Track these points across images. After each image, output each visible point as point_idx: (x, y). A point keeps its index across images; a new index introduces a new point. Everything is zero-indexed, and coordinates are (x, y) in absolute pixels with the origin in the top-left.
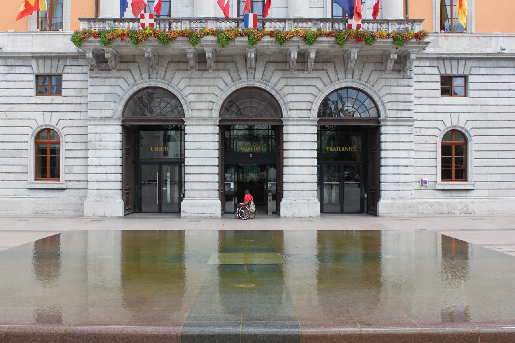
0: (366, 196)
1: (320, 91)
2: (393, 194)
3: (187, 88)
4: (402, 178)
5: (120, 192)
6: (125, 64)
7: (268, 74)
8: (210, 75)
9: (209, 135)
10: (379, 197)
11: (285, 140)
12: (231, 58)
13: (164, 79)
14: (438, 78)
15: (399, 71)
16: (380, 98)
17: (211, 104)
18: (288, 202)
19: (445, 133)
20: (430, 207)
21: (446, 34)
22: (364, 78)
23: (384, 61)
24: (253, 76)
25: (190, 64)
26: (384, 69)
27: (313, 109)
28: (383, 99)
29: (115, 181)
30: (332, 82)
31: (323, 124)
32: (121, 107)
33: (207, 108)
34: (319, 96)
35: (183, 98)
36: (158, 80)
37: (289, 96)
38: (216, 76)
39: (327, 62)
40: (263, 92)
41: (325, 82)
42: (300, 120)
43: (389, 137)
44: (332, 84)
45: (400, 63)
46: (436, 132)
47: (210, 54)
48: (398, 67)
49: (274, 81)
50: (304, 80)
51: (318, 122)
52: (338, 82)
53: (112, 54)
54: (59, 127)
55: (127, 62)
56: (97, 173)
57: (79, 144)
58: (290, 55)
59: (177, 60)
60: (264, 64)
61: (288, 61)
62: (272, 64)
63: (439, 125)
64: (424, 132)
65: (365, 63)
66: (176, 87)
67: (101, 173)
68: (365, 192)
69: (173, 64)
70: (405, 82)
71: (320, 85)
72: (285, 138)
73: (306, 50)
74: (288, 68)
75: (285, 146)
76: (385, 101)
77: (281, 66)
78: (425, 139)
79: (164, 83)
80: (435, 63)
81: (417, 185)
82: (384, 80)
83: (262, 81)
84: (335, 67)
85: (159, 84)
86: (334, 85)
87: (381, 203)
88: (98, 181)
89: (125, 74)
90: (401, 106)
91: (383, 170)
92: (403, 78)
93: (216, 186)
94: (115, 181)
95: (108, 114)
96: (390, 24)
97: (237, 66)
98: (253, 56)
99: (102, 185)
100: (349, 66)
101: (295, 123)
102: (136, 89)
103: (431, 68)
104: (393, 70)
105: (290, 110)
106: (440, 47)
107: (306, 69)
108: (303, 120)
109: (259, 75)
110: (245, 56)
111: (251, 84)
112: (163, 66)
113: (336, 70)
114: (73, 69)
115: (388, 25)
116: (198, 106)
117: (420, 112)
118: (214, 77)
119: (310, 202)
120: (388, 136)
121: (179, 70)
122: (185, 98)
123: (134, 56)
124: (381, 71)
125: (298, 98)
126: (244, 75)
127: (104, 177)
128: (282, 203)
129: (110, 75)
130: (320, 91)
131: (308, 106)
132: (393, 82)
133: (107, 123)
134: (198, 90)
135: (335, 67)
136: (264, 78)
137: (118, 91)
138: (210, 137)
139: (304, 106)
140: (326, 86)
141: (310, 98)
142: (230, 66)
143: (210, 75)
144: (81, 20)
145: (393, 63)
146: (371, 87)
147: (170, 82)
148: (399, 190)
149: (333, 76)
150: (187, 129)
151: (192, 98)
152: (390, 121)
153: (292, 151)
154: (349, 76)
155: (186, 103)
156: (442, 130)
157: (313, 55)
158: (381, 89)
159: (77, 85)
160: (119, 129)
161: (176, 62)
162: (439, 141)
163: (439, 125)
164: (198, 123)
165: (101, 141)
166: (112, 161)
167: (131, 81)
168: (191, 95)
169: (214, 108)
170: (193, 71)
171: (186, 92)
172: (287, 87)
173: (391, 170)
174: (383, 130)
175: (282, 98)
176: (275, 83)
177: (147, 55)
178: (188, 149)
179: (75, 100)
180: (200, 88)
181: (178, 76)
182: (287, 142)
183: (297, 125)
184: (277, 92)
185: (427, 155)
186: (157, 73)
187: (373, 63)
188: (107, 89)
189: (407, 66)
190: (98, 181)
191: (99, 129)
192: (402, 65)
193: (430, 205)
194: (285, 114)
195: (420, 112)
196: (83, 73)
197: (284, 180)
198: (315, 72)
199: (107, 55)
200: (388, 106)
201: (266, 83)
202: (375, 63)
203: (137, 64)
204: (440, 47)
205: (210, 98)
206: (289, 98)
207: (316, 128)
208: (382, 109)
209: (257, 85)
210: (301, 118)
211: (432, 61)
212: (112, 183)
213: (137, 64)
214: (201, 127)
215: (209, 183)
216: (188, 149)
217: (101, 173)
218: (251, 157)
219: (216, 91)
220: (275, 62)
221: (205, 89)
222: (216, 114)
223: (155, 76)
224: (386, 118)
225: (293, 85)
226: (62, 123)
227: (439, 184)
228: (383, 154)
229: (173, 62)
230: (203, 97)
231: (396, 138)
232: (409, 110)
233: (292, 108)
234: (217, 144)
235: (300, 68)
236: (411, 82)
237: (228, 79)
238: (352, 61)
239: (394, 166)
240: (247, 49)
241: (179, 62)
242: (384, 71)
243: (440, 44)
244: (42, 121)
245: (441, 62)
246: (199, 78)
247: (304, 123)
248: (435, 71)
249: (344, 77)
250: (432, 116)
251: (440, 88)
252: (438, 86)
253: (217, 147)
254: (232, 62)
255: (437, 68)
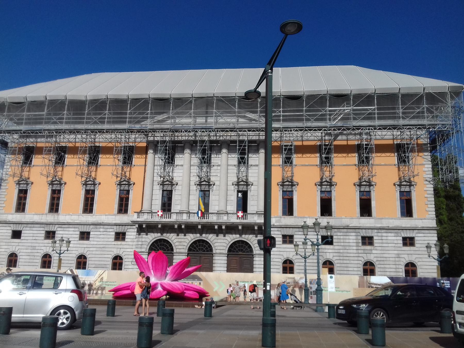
46: (280, 260)
54: (123, 255)
75: (214, 265)
114: (131, 230)
116: (180, 247)
134: (180, 240)
144: (135, 212)
151: (177, 244)
159: (132, 237)
171: (175, 241)
179: (130, 243)
206: (216, 244)
210: (220, 254)
226: (124, 253)
230: (181, 244)
244: (116, 252)
248: (279, 233)
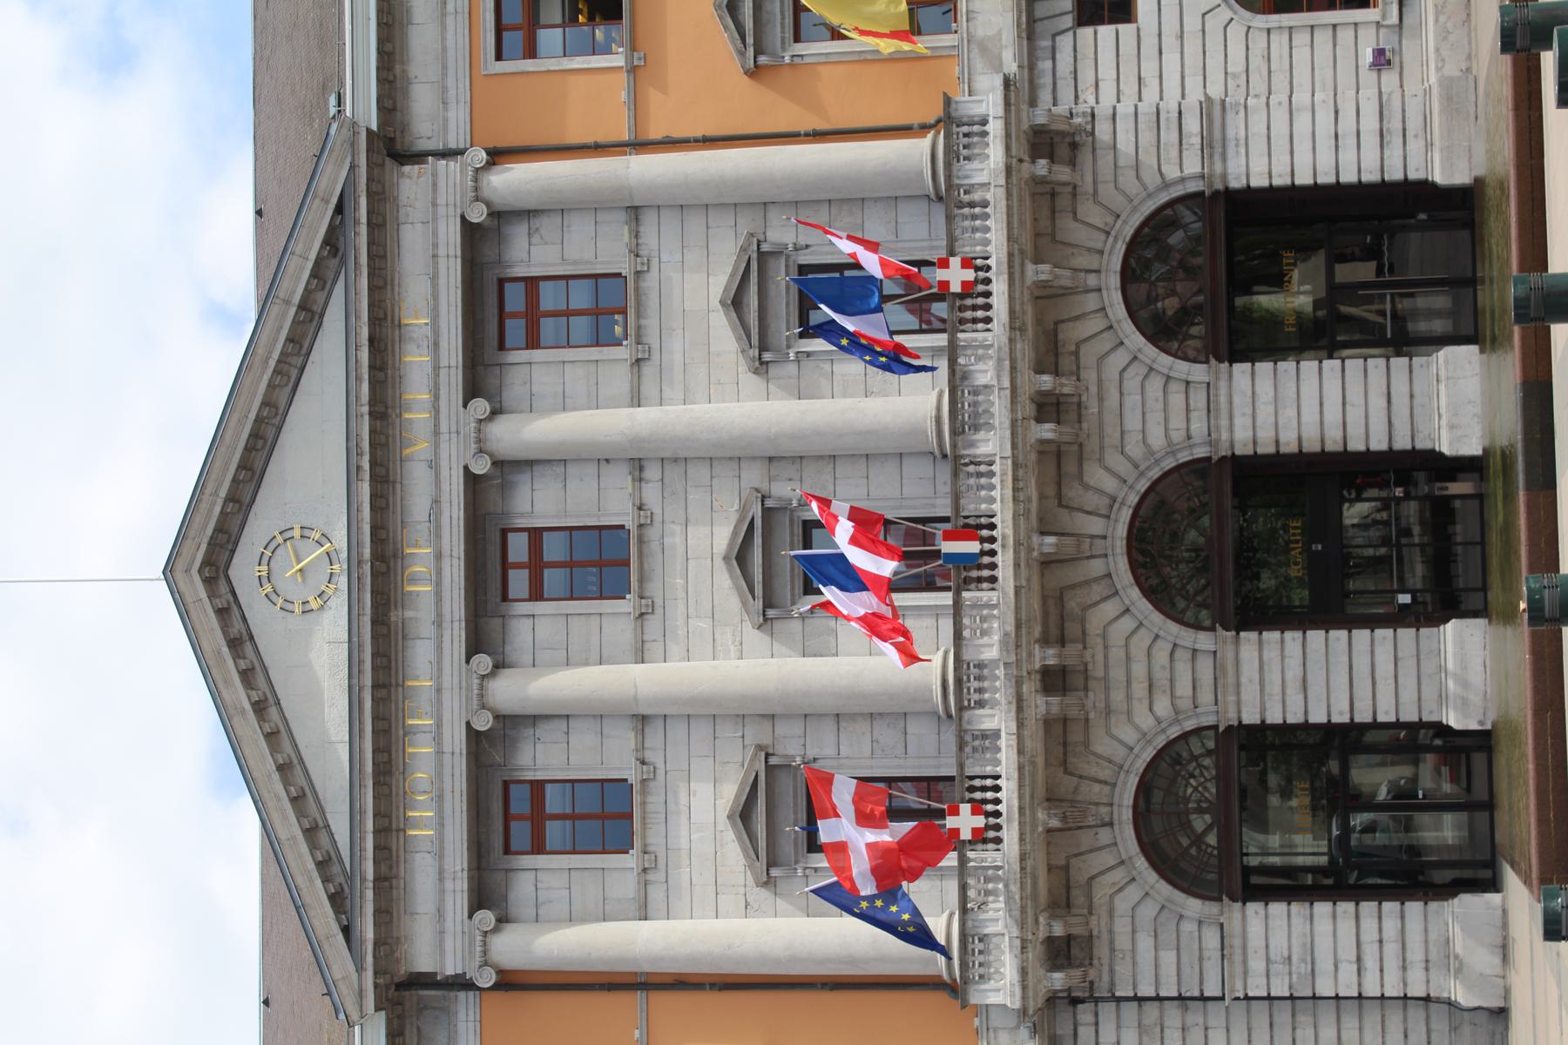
0: (1422, 216)
1: (1135, 358)
2: (1415, 146)
3: (1137, 720)
4: (1370, 123)
5: (1433, 905)
6: (1075, 892)
7: (1092, 501)
8: (1100, 658)
9: (1265, 657)
10: (1425, 186)
11: (1271, 450)
12: (1051, 602)
13: (1114, 785)
14: (1086, 32)
15: (1074, 146)
16: (1150, 196)
17: (1179, 653)
18: (1444, 433)
19: (1237, 7)
20: (1452, 38)
21: (962, 18)
22: (1096, 240)
23: (1047, 188)
24: (1098, 542)
25: (1074, 712)
26: (1070, 189)
27: (1184, 377)
28: (1151, 188)
29: (1402, 917)
30: (1111, 327)
31: (1224, 347)
32: (1194, 906)
33: (1189, 665)
34: (1148, 361)
35: (1164, 731)
36: (1116, 801)
37: (1151, 441)
38: (1099, 640)
39: (1056, 343)
40: (1142, 513)
41: (1108, 346)
42: (1217, 410)
43: (1257, 165)
44: (1115, 326)
45: (1052, 145)
46: (1236, 33)
47: (1051, 652)
48: (1063, 151)
49: (1110, 484)
50: (1106, 404)
51: (1221, 361)
52: (1109, 310)
53: (1052, 917)
55: (1068, 888)
56: (1381, 970)
57: (1298, 1032)
58: (1042, 442)
59: (1061, 748)
60: (1064, 512)
61: (1053, 448)
62: (1065, 490)
63: (1215, 23)
64: (1237, 65)
65: (1054, 240)
66: (1136, 751)
67: (1381, 960)
68: (1414, 216)
69: (1071, 759)
70: (1103, 130)
71: (1119, 359)
72: (1266, 448)
73: (1032, 400)
74: (1075, 448)
75: (1289, 447)
76: (1159, 180)
77: (1070, 467)
78: (1257, 61)
79: (1125, 783)
80: (1046, 43)
81: (1390, 78)
82: (1101, 187)
83: (1113, 516)
84: (1069, 320)
85: (1126, 796)
86: (1119, 322)
87: (1439, 178)
88: (1404, 968)
89: (1100, 894)
90: (1170, 136)
91: (1349, 177)
92: (1093, 133)
93: (1406, 634)
94: (1402, 917)
95: (1211, 939)
96: (957, 181)
97: (1073, 587)
98: (1051, 540)
99: (1416, 954)
100: (1067, 283)
101: (1224, 422)
102: (1141, 863)
103: (1058, 56)
104: (1072, 163)
105: (1189, 437)
106: (1000, 31)
107: (1075, 400)
108: (1217, 402)
109: (1095, 526)
110: (1047, 563)
111: (1120, 546)
112: (1076, 788)
113: (1077, 318)
115: (960, 186)
116: (1184, 688)
117: (1183, 77)
118: (1106, 647)
119: (1442, 374)
120: (1254, 169)
121: (1086, 744)
122: (1163, 725)
123: (1049, 870)
124: (1074, 195)
125: (1155, 417)
126: (1096, 567)
127: (1391, 949)
128: (1446, 450)
129: (1105, 936)
130: (1135, 358)
131: (1176, 389)
132: (1105, 161)
133: (1237, 942)
134: (1140, 689)
135: (1069, 320)
136: (1103, 512)
137: (1148, 911)
138: (1272, 653)
139: (1177, 400)
140: (1122, 343)
141: (1155, 385)
142: (1072, 604)
143: (1100, 658)
145: (1056, 168)
146: (1119, 222)
147: (1121, 767)
148: (1404, 130)
149: (1094, 325)
150: (1250, 717)
151: (1163, 706)
152: (1212, 164)
153: (1303, 427)
154: (1092, 280)
155: (1177, 721)
156: (1228, 14)
157: (1046, 382)
158: (1124, 194)
160: (1254, 908)
161: (1065, 754)
162: (1262, 21)
163: (1215, 23)
164: (1231, 689)
165: (1289, 958)
166: (1346, 927)
167: (1118, 875)
168: (1155, 708)
169: (1189, 644)
170: (1089, 703)
171: (1145, 721)
172: (1127, 449)
173: (1348, 157)
174: (1236, 183)
175: (1157, 461)
176: (1115, 485)
177: (1055, 823)
178: (1306, 712)
180: (1135, 685)
181: (1102, 745)
182: (1277, 442)
183: (1231, 418)
184: (1142, 474)
185: (1302, 54)
186: (1097, 804)
187: (1053, 219)
188: (1145, 943)
189: (1064, 127)
190: (1404, 968)
191: (1257, 965)
192: (1057, 139)
193: (1445, 39)
194: (1201, 452)
195: (1183, 77)
196: (1097, 1024)
197: (1384, 447)
198: (1083, 374)
199: (1058, 930)
200: (1172, 172)
201: (1116, 506)
202: (1053, 212)
203: (1073, 861)
204: (1000, 31)
205: (1161, 655)
206: (1157, 439)
207: (1236, 366)
208: (1180, 187)
209: (1122, 530)
211: (1039, 53)
212: (1408, 926)
213: (1073, 861)
214: (1243, 680)
215: (1400, 654)
216: (1306, 712)
217: (1381, 960)
218: (1320, 547)
219: (1142, 641)
220: (1059, 484)
221: (1139, 669)
222: (1204, 641)
223: (1104, 810)
224: (1202, 176)
225: (1122, 432)
227: (1384, 17)
228: (1304, 179)
229: (1065, 762)
230: (1161, 676)
231: (1258, 146)
232: (1180, 113)
233: (1183, 433)
234: (1289, 635)
235: (1073, 416)
236: (1103, 110)
237: (1110, 609)
238: (1056, 277)
239: (1337, 147)
240: (1035, 554)
241: (1065, 744)
242: (1075, 187)
243: (990, 33)
245: (1039, 27)
246: (1107, 689)
247: (1223, 399)
248: (1065, 42)
249: (1093, 296)
250: (1192, 46)
251: (1112, 28)
252: (1106, 31)
253: (1298, 635)
254: (1061, 598)
255: (1058, 38)
